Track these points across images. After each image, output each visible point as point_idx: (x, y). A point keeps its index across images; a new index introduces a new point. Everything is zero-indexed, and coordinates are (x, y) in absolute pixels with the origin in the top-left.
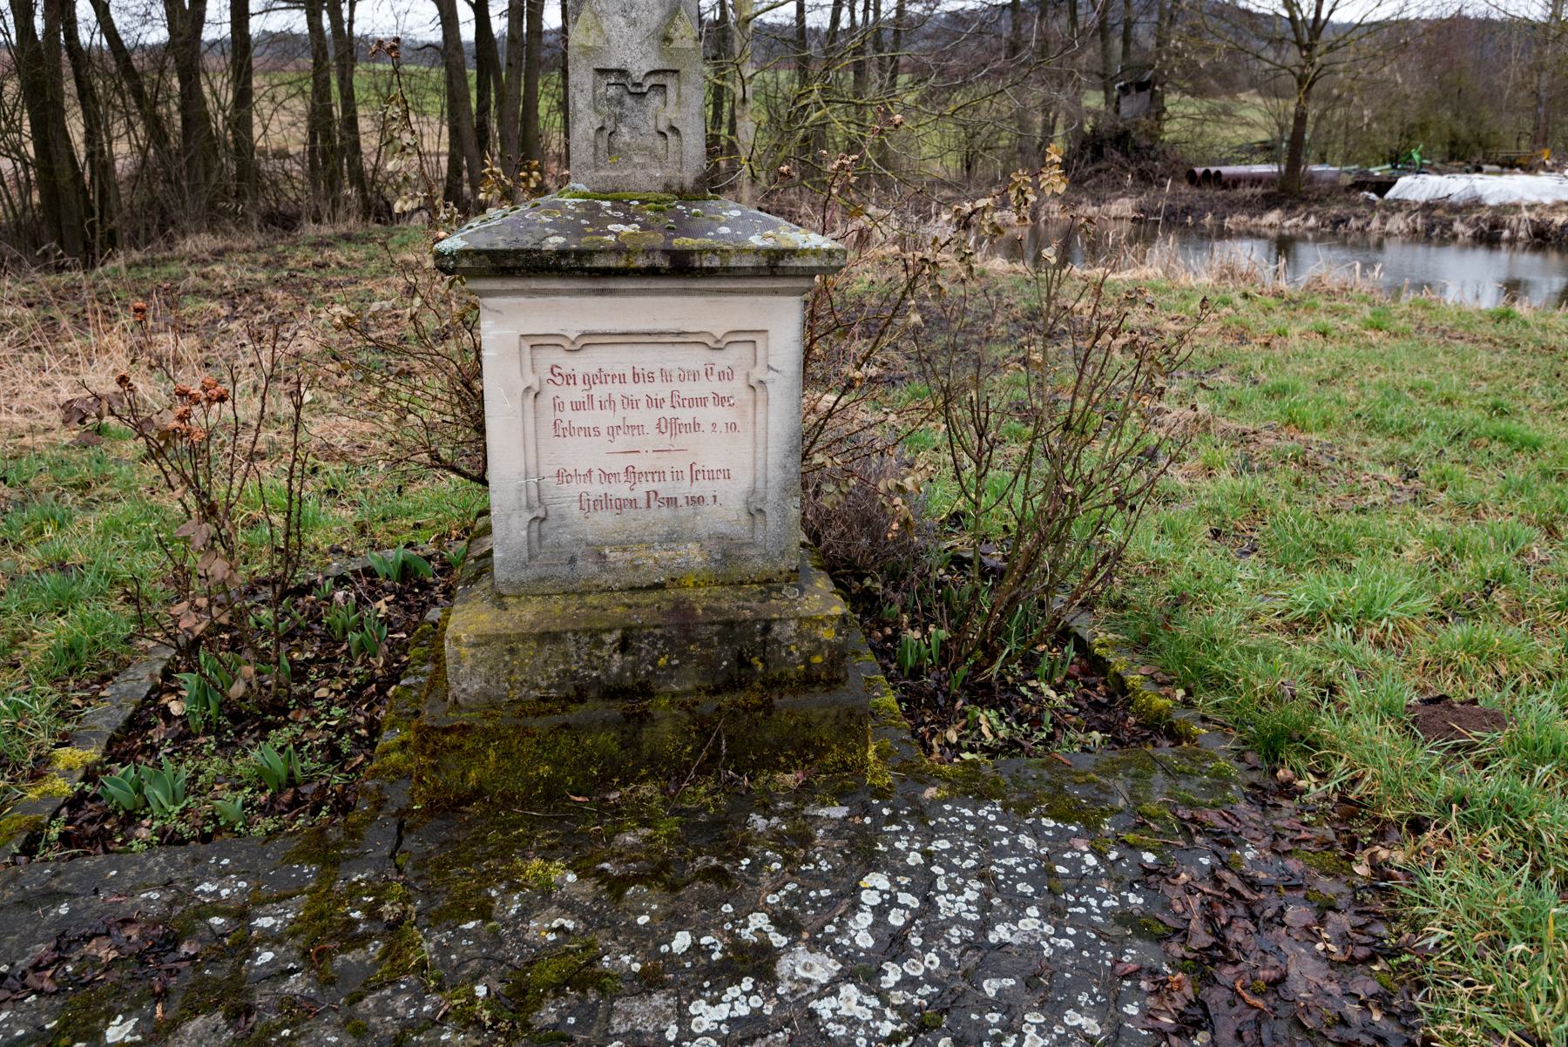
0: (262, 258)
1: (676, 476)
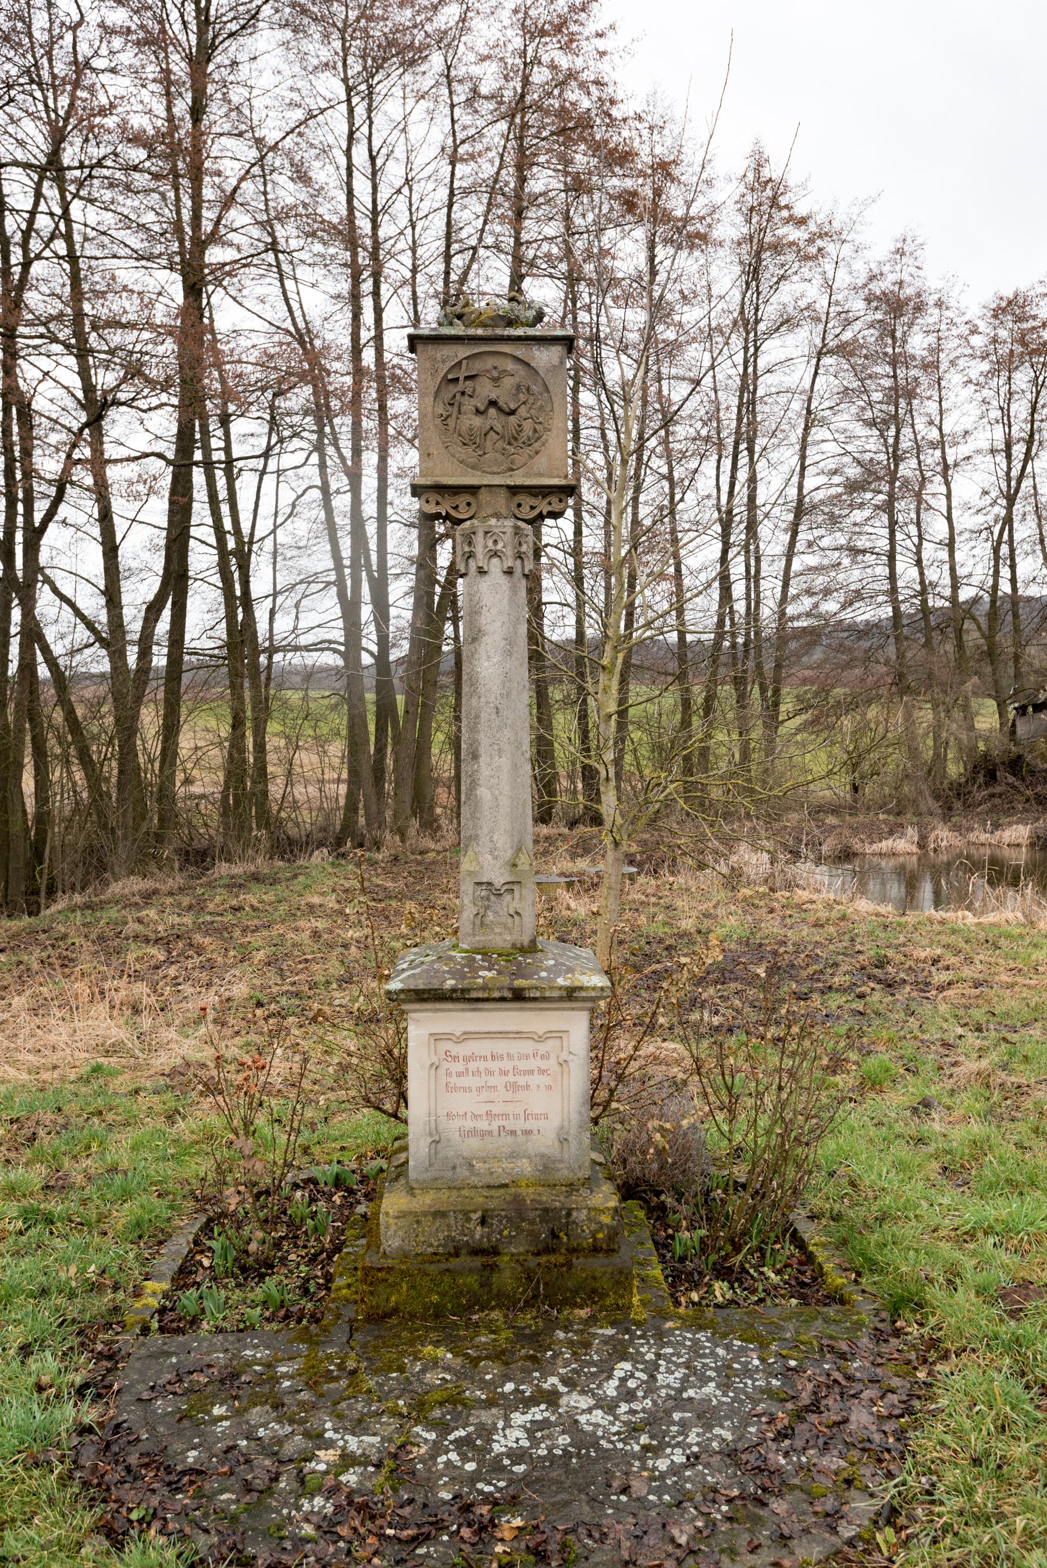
0: (186, 901)
1: (516, 1117)
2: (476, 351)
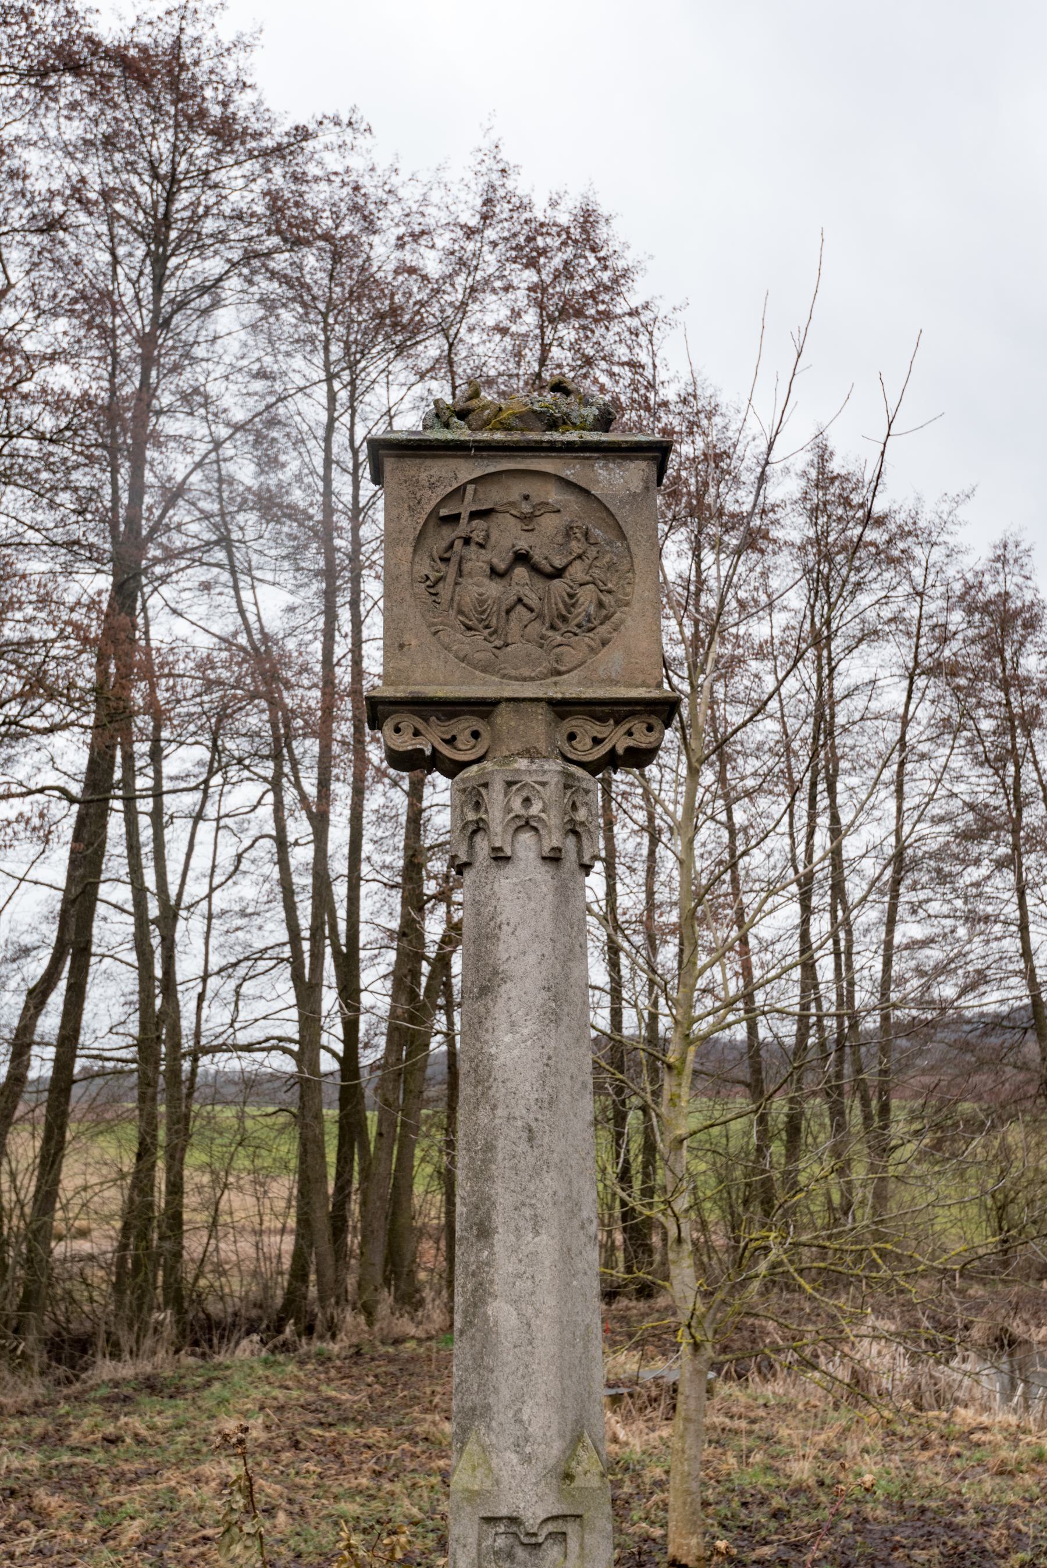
0: (39, 1425)
2: (491, 469)
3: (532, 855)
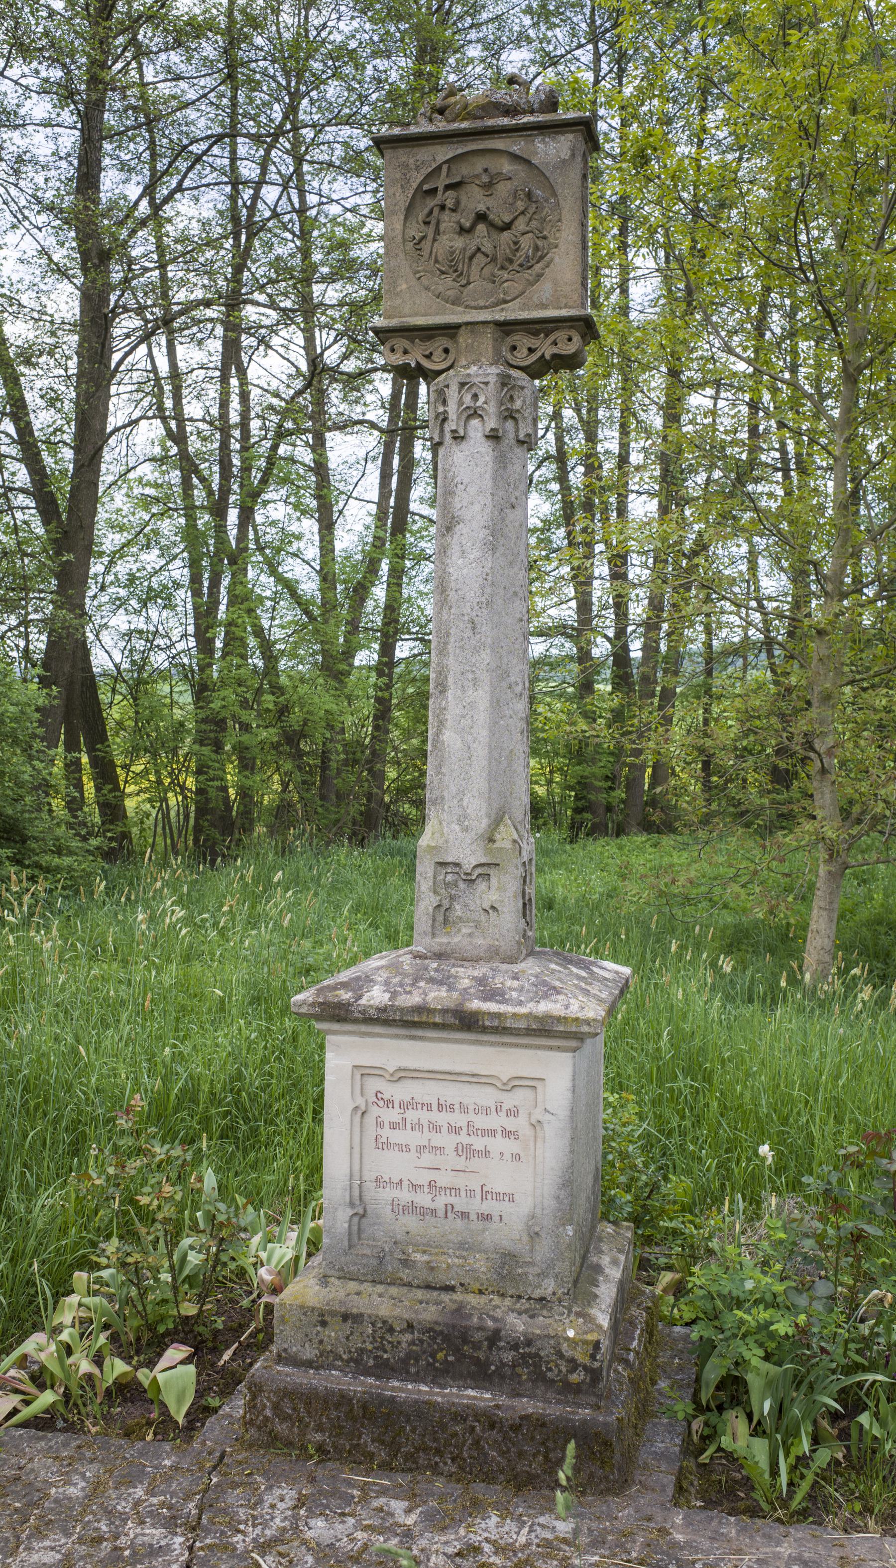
1: (471, 1193)
2: (460, 151)
3: (480, 435)
